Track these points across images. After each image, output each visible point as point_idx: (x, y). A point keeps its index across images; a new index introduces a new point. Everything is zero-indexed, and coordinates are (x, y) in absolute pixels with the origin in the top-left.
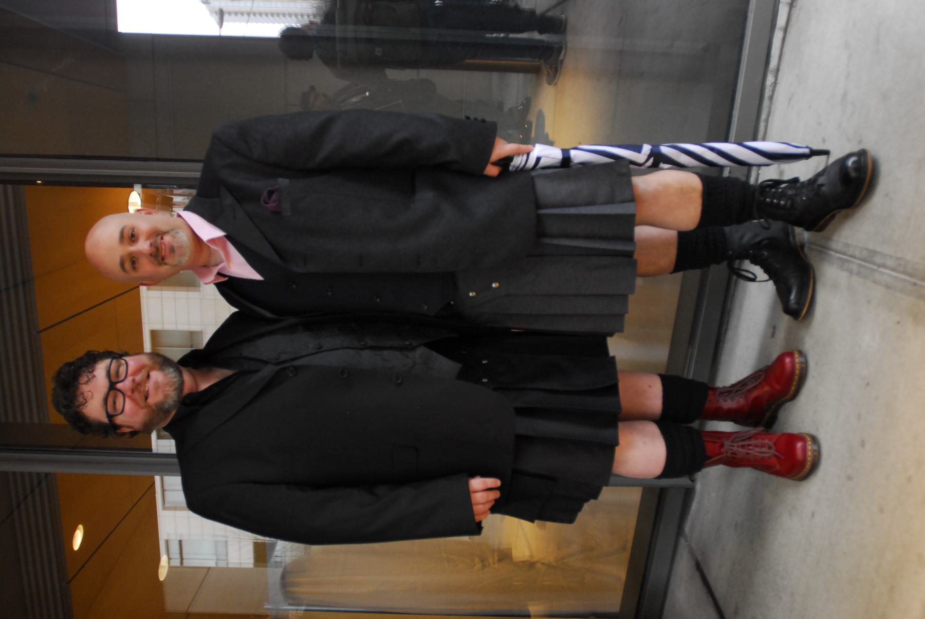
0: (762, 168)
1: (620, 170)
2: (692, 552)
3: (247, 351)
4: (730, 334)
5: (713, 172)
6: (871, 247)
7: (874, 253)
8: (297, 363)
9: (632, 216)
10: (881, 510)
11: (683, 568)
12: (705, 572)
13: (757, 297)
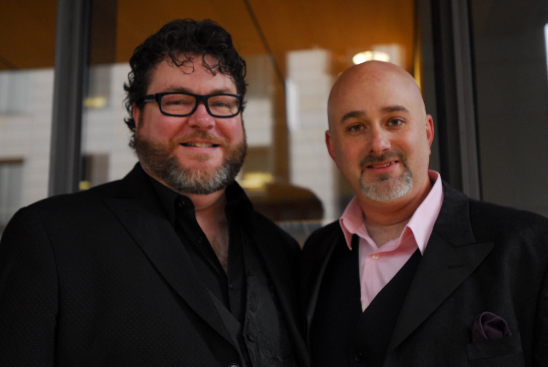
3: (256, 286)
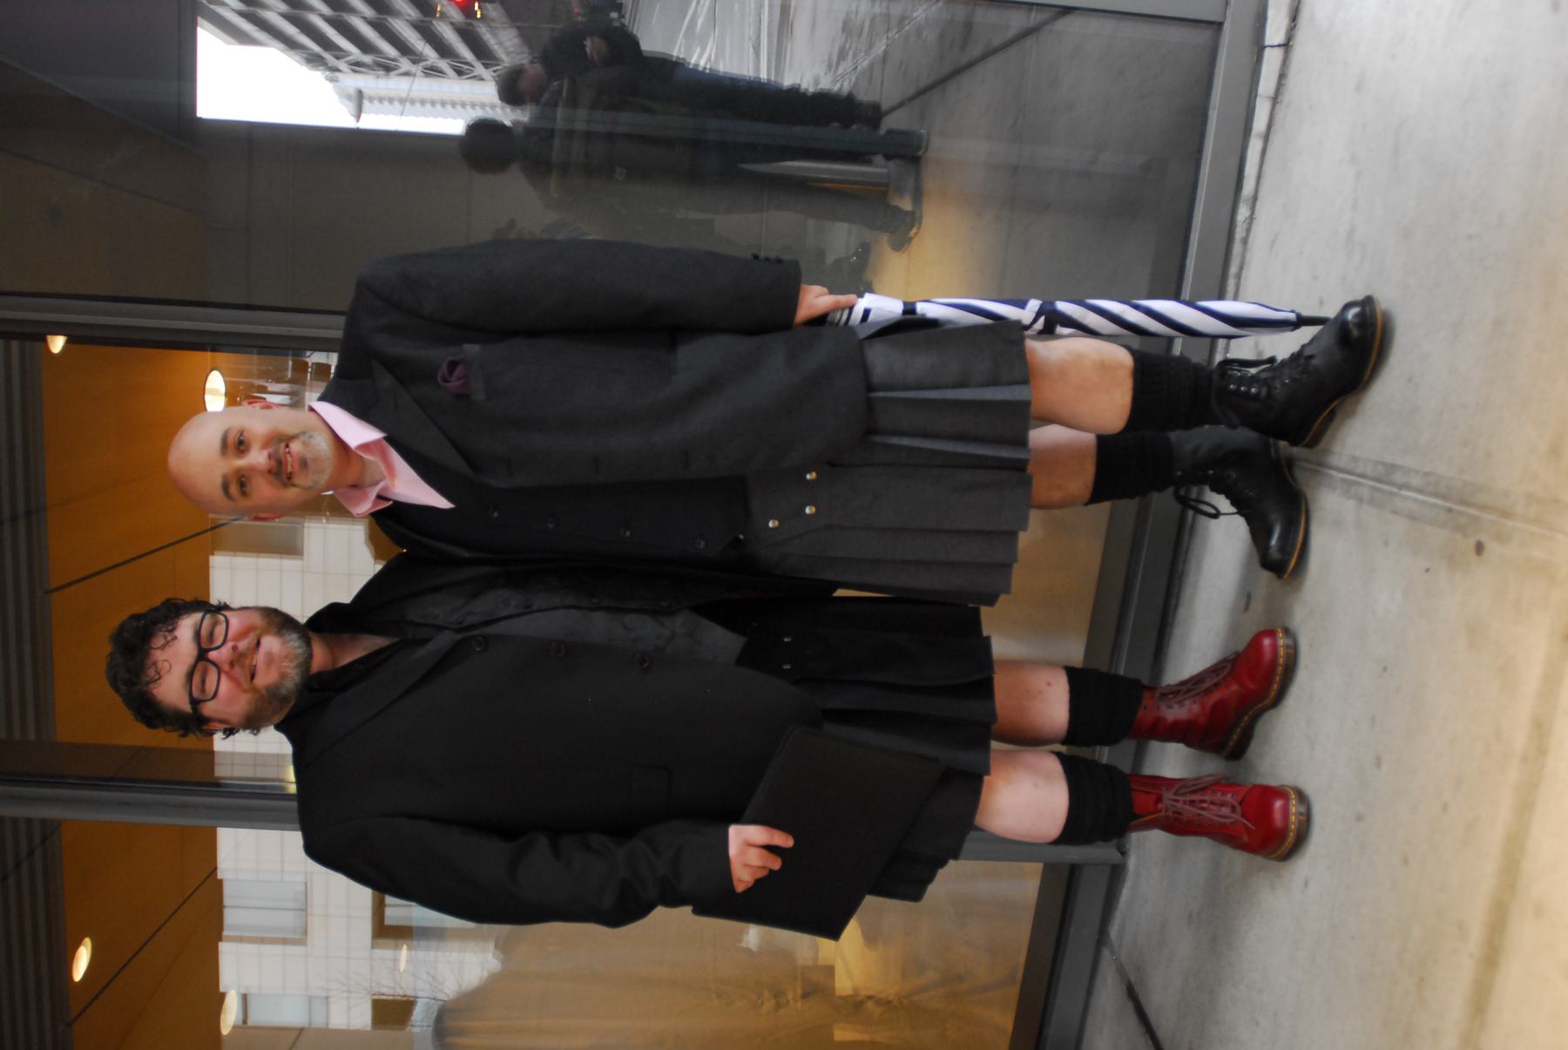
0: (1233, 341)
1: (1005, 335)
2: (1121, 970)
4: (1182, 611)
5: (1154, 348)
6: (1388, 459)
7: (1393, 467)
8: (491, 630)
9: (1026, 404)
10: (1406, 861)
11: (1108, 995)
12: (1143, 1001)
13: (1224, 540)
